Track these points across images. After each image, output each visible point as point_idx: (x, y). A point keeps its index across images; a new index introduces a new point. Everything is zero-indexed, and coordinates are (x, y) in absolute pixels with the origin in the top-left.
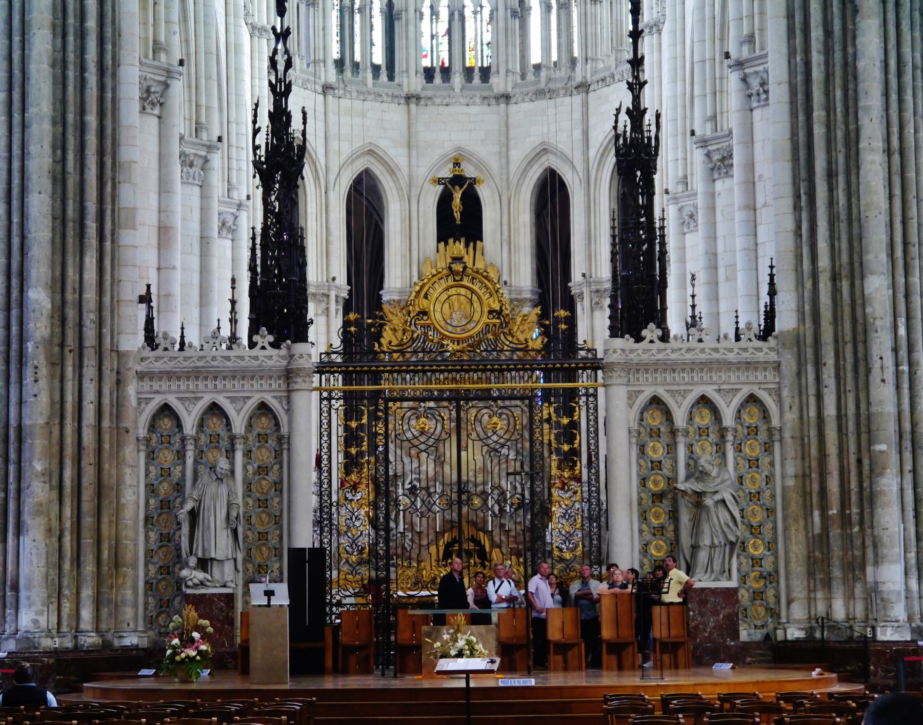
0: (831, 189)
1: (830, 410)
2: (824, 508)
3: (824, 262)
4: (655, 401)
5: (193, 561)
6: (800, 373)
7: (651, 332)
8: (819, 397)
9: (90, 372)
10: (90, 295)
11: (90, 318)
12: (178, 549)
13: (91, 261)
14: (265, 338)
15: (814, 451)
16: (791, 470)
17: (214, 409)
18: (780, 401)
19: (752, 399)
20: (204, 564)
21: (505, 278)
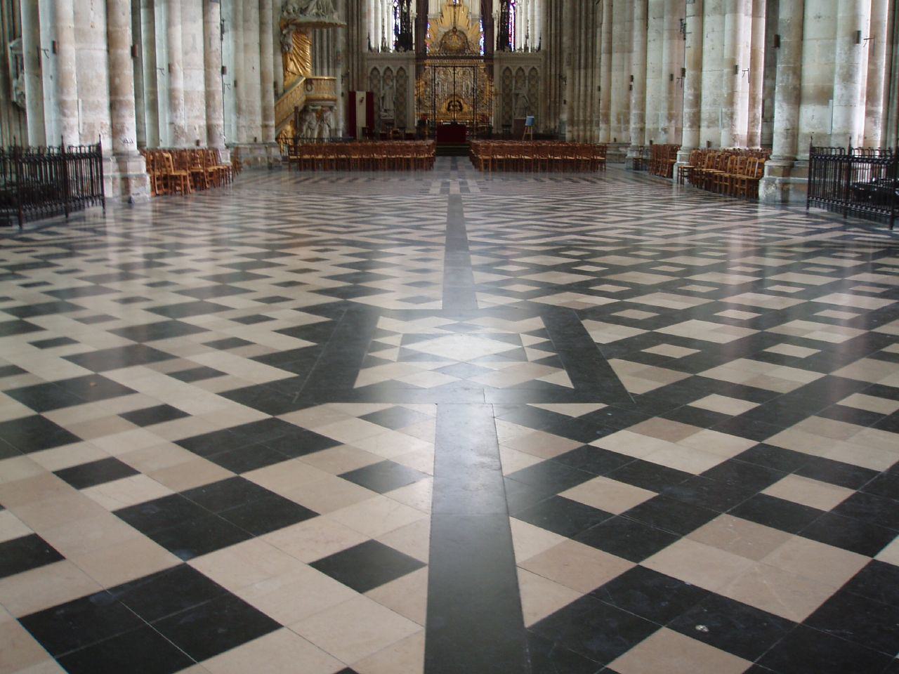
0: (556, 12)
1: (553, 73)
2: (550, 99)
3: (553, 32)
4: (508, 68)
5: (383, 110)
6: (546, 62)
7: (507, 49)
8: (551, 68)
9: (355, 57)
10: (355, 38)
11: (355, 44)
12: (379, 107)
13: (355, 28)
14: (402, 49)
15: (548, 83)
16: (542, 88)
17: (388, 68)
18: (540, 69)
19: (534, 68)
20: (386, 111)
21: (470, 11)
